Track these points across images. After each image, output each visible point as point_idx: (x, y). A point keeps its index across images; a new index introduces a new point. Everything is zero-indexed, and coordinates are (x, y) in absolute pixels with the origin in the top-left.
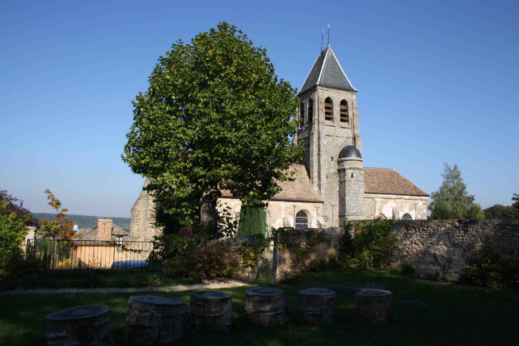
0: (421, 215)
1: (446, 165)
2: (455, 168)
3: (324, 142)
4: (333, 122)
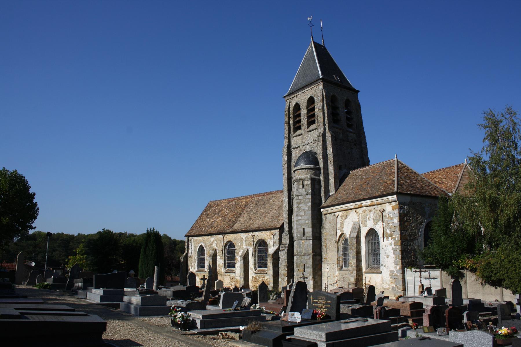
0: (390, 228)
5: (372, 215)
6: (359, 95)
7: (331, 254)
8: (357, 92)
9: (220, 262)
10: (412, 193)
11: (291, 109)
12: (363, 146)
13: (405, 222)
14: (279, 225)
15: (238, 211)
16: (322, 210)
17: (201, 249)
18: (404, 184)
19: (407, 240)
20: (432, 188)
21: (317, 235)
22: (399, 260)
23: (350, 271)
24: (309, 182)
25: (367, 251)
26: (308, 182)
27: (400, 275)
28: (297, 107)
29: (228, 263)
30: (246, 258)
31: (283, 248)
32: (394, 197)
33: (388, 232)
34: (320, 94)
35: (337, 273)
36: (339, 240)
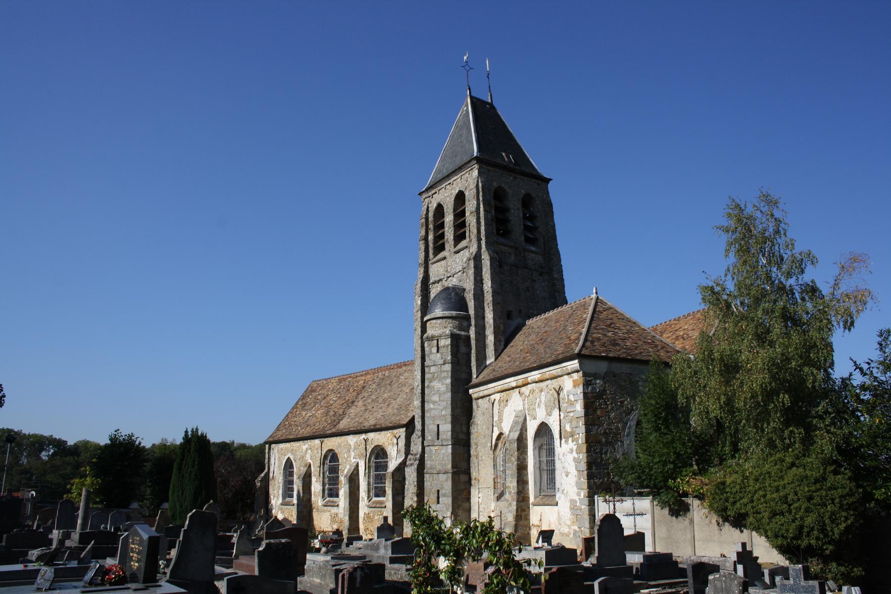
5: (543, 398)
6: (551, 186)
7: (483, 470)
8: (548, 181)
9: (316, 487)
10: (611, 355)
11: (431, 215)
12: (556, 276)
13: (596, 409)
14: (405, 421)
15: (350, 396)
16: (471, 391)
17: (289, 465)
18: (599, 339)
19: (600, 442)
20: (656, 346)
21: (462, 436)
22: (584, 481)
23: (508, 501)
24: (449, 341)
25: (538, 465)
26: (446, 342)
27: (585, 508)
28: (440, 209)
29: (330, 490)
30: (353, 479)
31: (412, 462)
32: (574, 364)
33: (568, 428)
34: (473, 186)
35: (493, 505)
36: (496, 445)
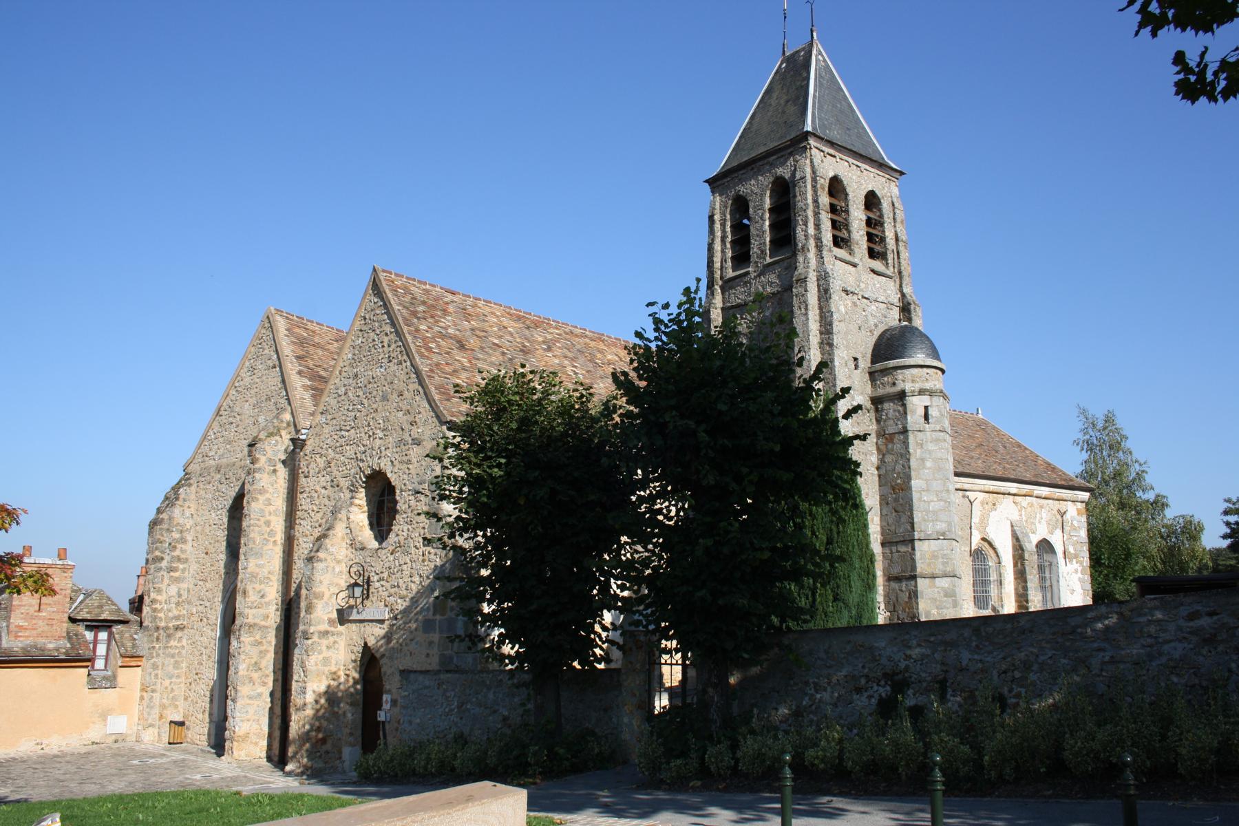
1: (1084, 412)
2: (1109, 420)
3: (840, 305)
4: (851, 253)
33: (1071, 549)
